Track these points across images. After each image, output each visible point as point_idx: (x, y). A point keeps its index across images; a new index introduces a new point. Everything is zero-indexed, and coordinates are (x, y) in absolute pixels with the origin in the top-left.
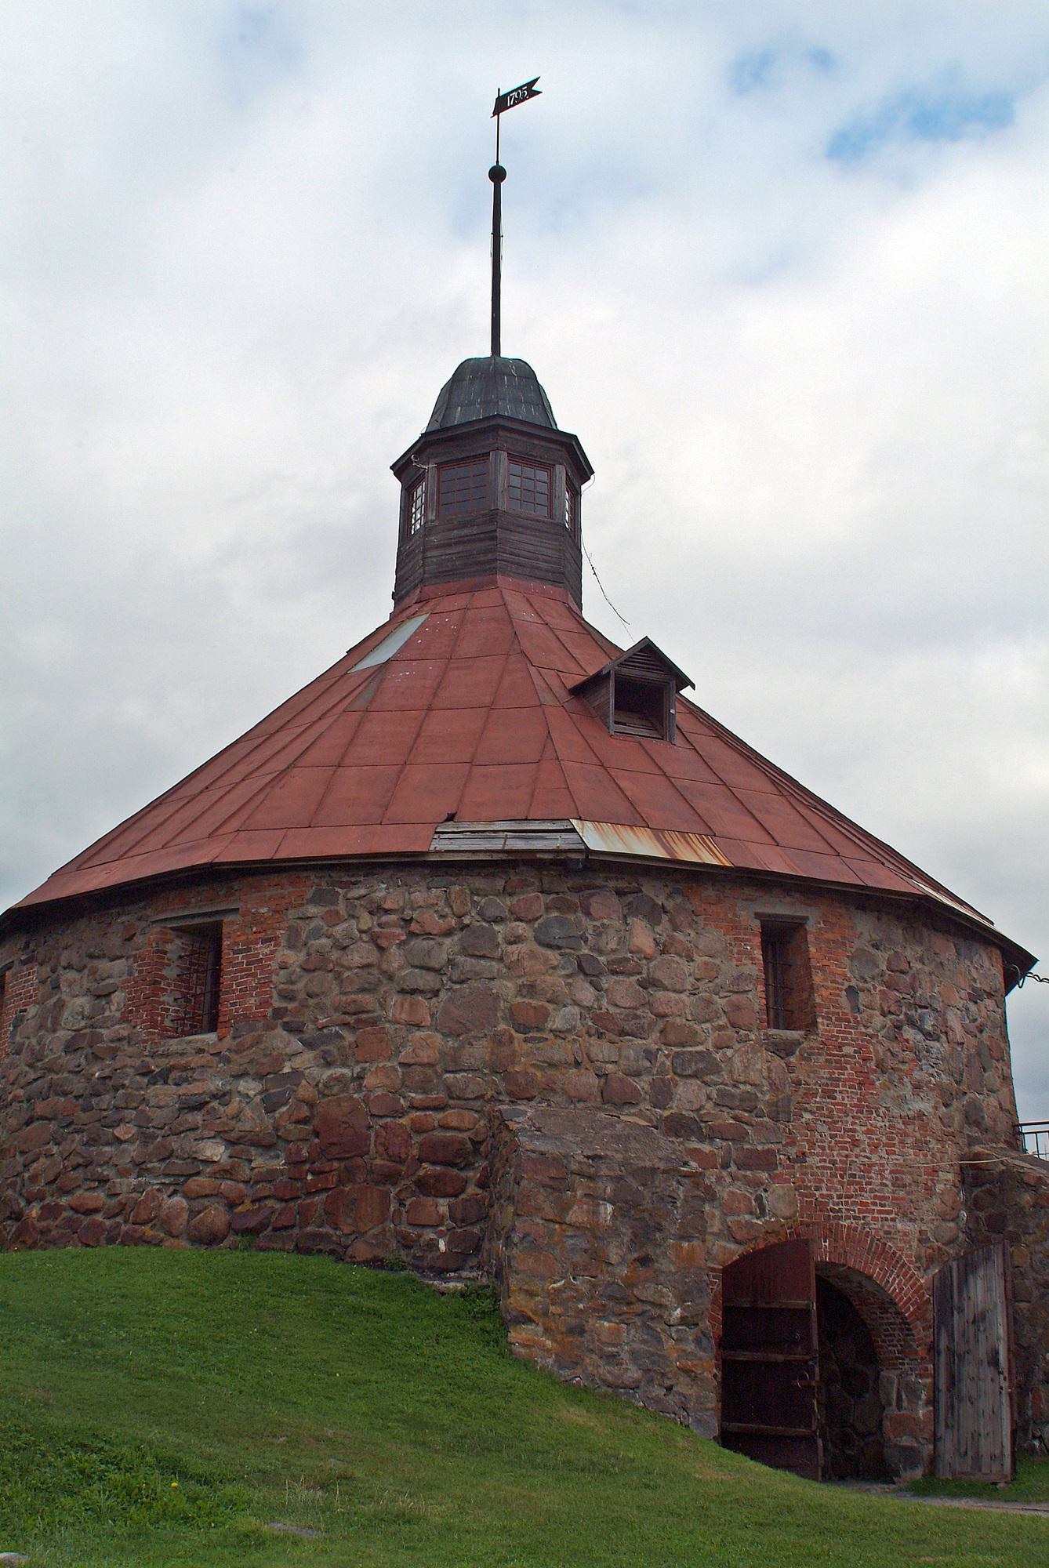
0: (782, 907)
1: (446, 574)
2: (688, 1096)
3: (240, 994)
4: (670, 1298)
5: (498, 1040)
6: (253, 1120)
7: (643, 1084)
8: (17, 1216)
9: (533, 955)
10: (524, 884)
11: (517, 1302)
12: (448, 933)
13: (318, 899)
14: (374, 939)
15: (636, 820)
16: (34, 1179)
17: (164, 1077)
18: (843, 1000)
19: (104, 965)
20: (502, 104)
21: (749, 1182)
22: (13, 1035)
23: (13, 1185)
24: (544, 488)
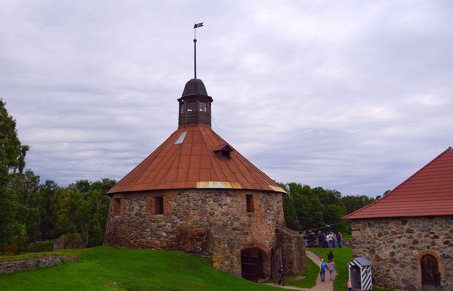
0: (249, 193)
1: (189, 123)
2: (236, 224)
3: (166, 209)
4: (235, 257)
5: (207, 217)
6: (170, 230)
8: (129, 242)
9: (212, 204)
10: (211, 192)
11: (214, 259)
12: (199, 200)
13: (179, 194)
14: (188, 201)
15: (227, 181)
16: (131, 236)
17: (154, 221)
18: (259, 208)
19: (141, 201)
20: (196, 26)
21: (245, 237)
22: (123, 211)
23: (127, 237)
24: (205, 106)
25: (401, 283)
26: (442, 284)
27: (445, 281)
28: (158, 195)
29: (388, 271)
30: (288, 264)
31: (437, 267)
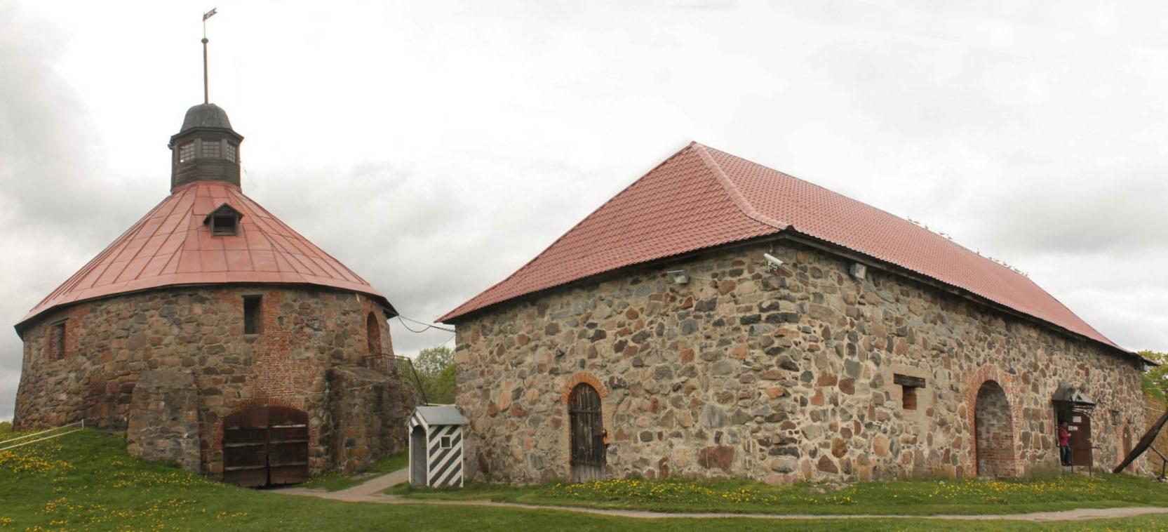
2: (212, 361)
7: (196, 359)
18: (277, 322)
25: (530, 466)
26: (609, 459)
27: (614, 452)
29: (508, 438)
30: (347, 445)
31: (598, 416)
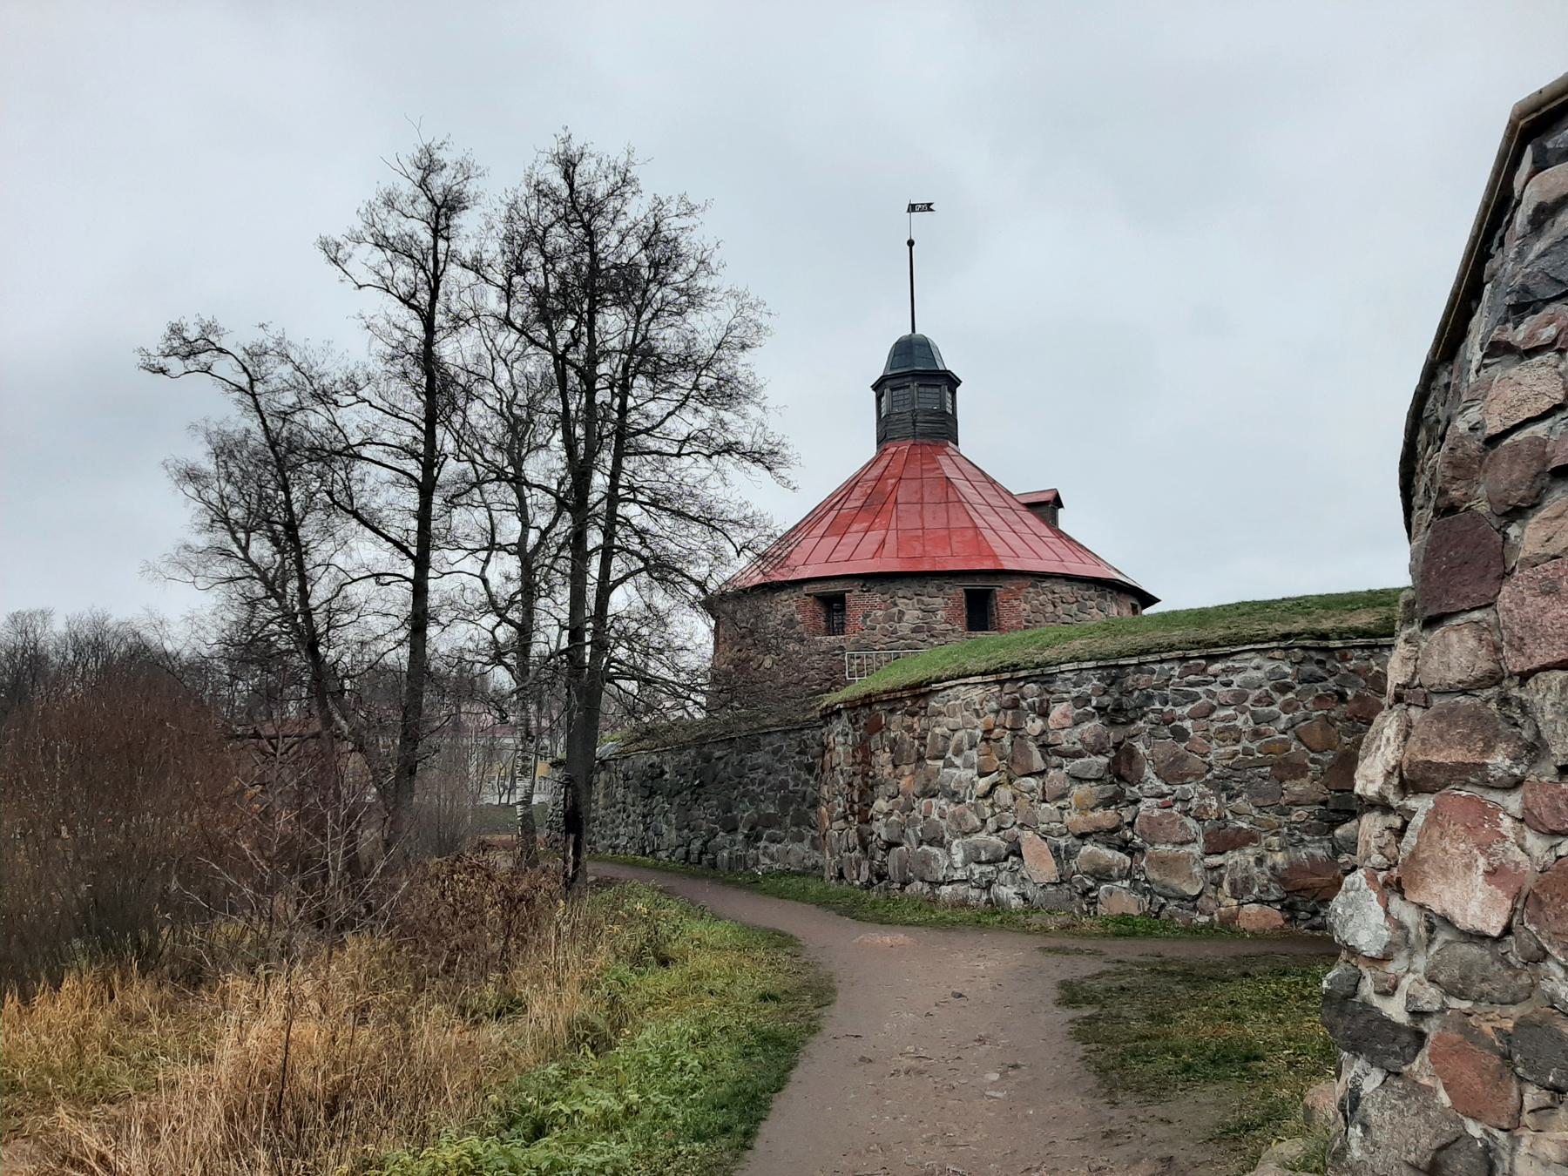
20: (912, 208)
22: (864, 622)
28: (979, 584)
